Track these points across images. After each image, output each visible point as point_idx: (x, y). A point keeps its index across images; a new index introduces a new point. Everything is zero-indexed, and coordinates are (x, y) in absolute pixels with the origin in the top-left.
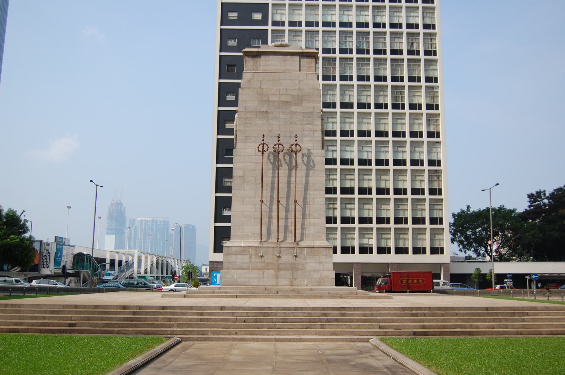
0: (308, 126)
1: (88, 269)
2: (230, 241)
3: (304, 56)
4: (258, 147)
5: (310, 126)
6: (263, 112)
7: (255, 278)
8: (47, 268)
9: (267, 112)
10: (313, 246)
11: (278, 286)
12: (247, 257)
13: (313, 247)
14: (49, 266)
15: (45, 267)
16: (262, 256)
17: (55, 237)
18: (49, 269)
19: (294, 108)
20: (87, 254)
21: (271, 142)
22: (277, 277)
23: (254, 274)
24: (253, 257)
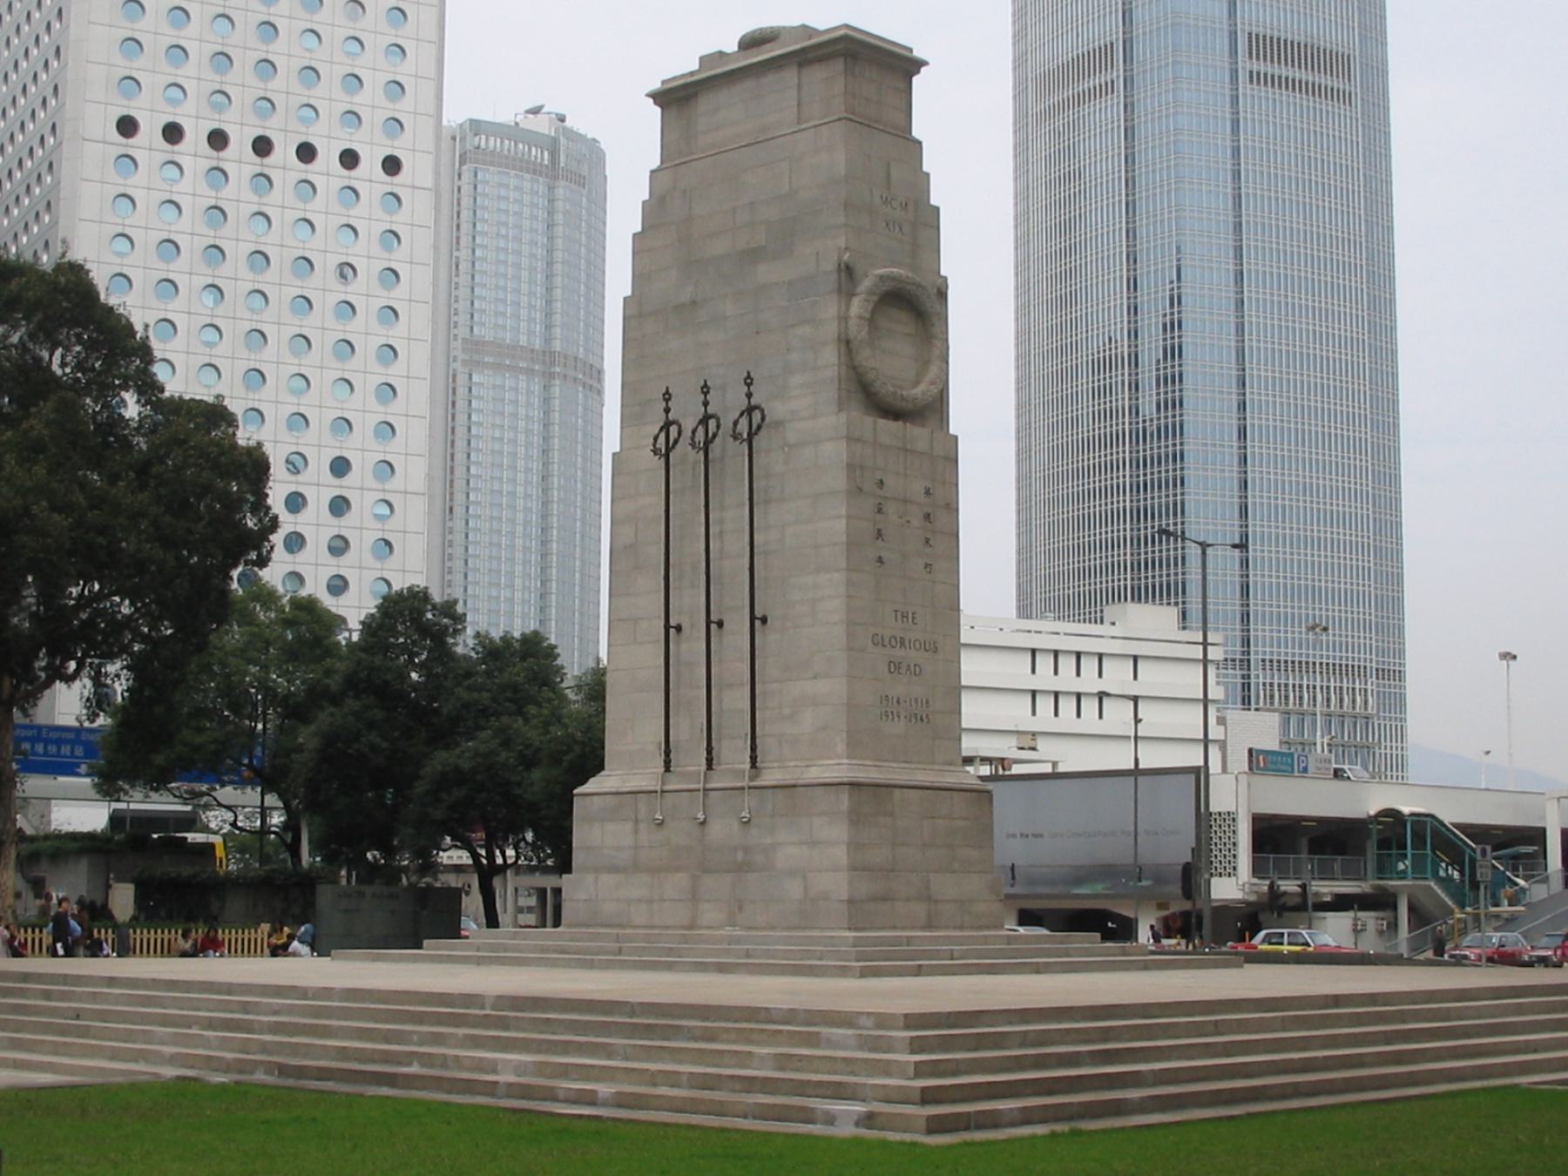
0: (800, 331)
1: (1429, 876)
2: (602, 773)
3: (811, 62)
4: (656, 439)
5: (805, 330)
6: (684, 305)
7: (640, 901)
8: (1230, 875)
9: (694, 303)
10: (792, 782)
11: (700, 928)
12: (629, 826)
13: (794, 786)
14: (1235, 868)
15: (1222, 871)
16: (661, 824)
17: (1250, 751)
18: (1233, 878)
19: (766, 273)
20: (1413, 814)
21: (688, 413)
22: (694, 897)
23: (637, 887)
24: (642, 826)
